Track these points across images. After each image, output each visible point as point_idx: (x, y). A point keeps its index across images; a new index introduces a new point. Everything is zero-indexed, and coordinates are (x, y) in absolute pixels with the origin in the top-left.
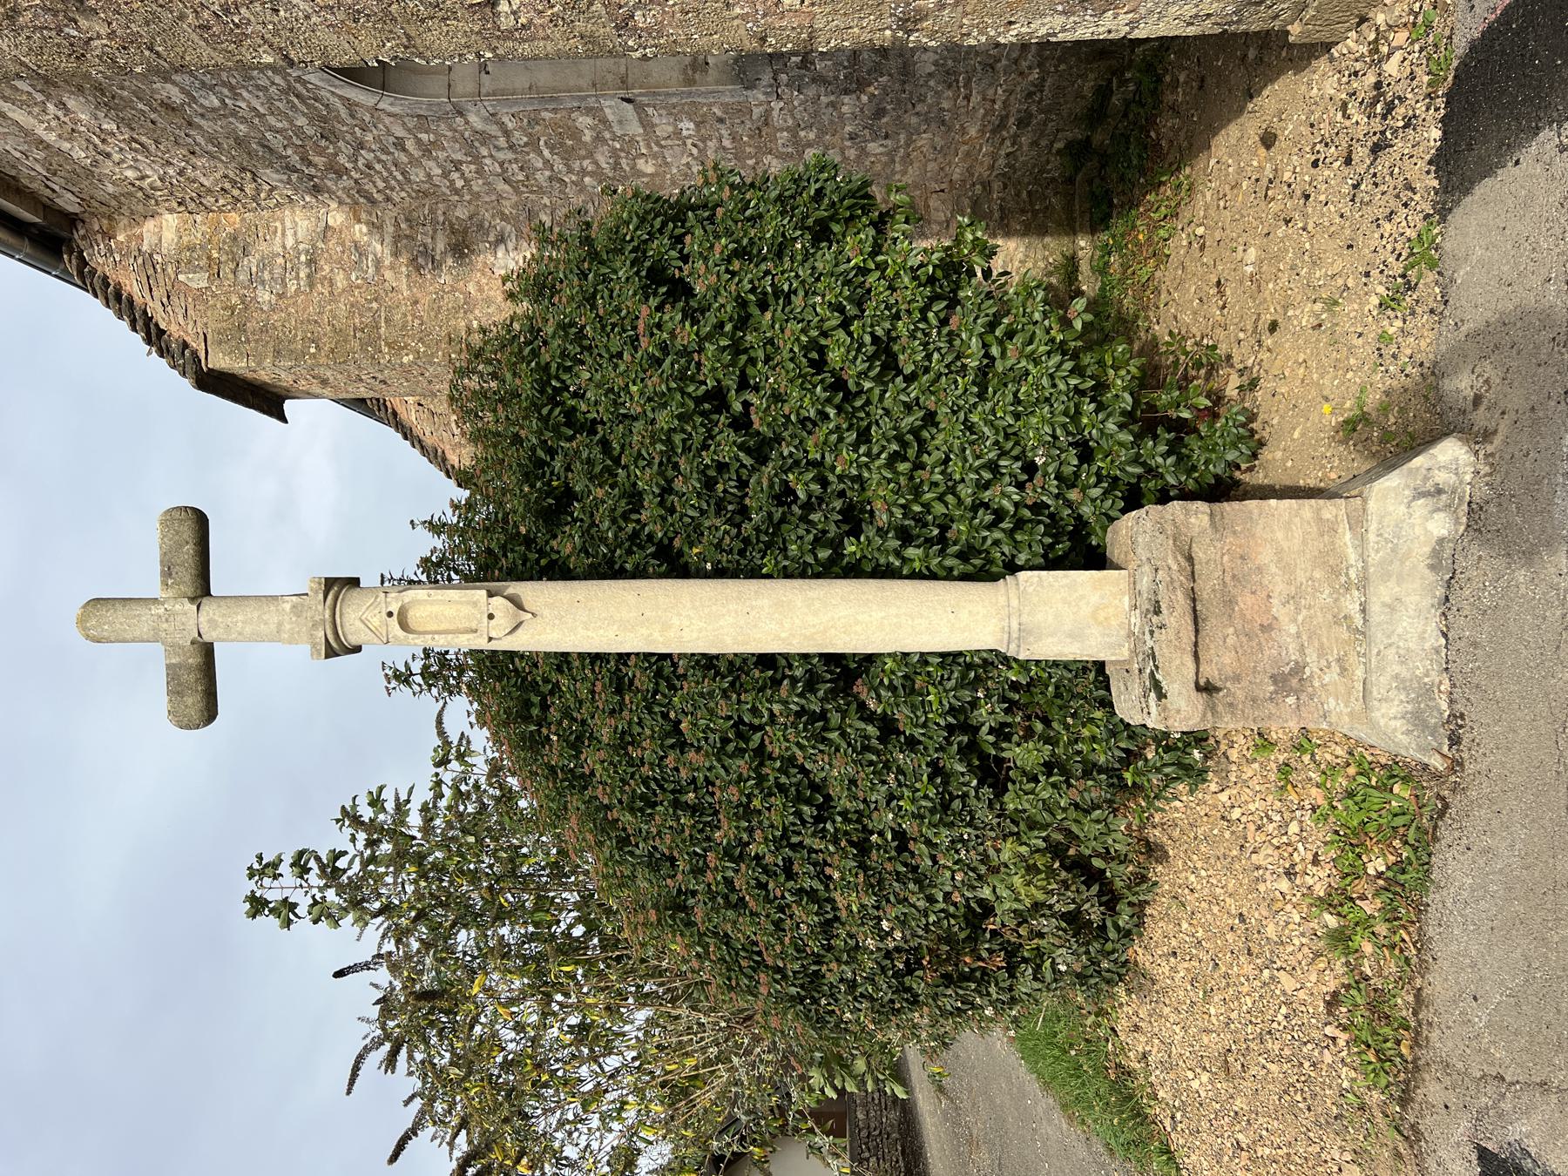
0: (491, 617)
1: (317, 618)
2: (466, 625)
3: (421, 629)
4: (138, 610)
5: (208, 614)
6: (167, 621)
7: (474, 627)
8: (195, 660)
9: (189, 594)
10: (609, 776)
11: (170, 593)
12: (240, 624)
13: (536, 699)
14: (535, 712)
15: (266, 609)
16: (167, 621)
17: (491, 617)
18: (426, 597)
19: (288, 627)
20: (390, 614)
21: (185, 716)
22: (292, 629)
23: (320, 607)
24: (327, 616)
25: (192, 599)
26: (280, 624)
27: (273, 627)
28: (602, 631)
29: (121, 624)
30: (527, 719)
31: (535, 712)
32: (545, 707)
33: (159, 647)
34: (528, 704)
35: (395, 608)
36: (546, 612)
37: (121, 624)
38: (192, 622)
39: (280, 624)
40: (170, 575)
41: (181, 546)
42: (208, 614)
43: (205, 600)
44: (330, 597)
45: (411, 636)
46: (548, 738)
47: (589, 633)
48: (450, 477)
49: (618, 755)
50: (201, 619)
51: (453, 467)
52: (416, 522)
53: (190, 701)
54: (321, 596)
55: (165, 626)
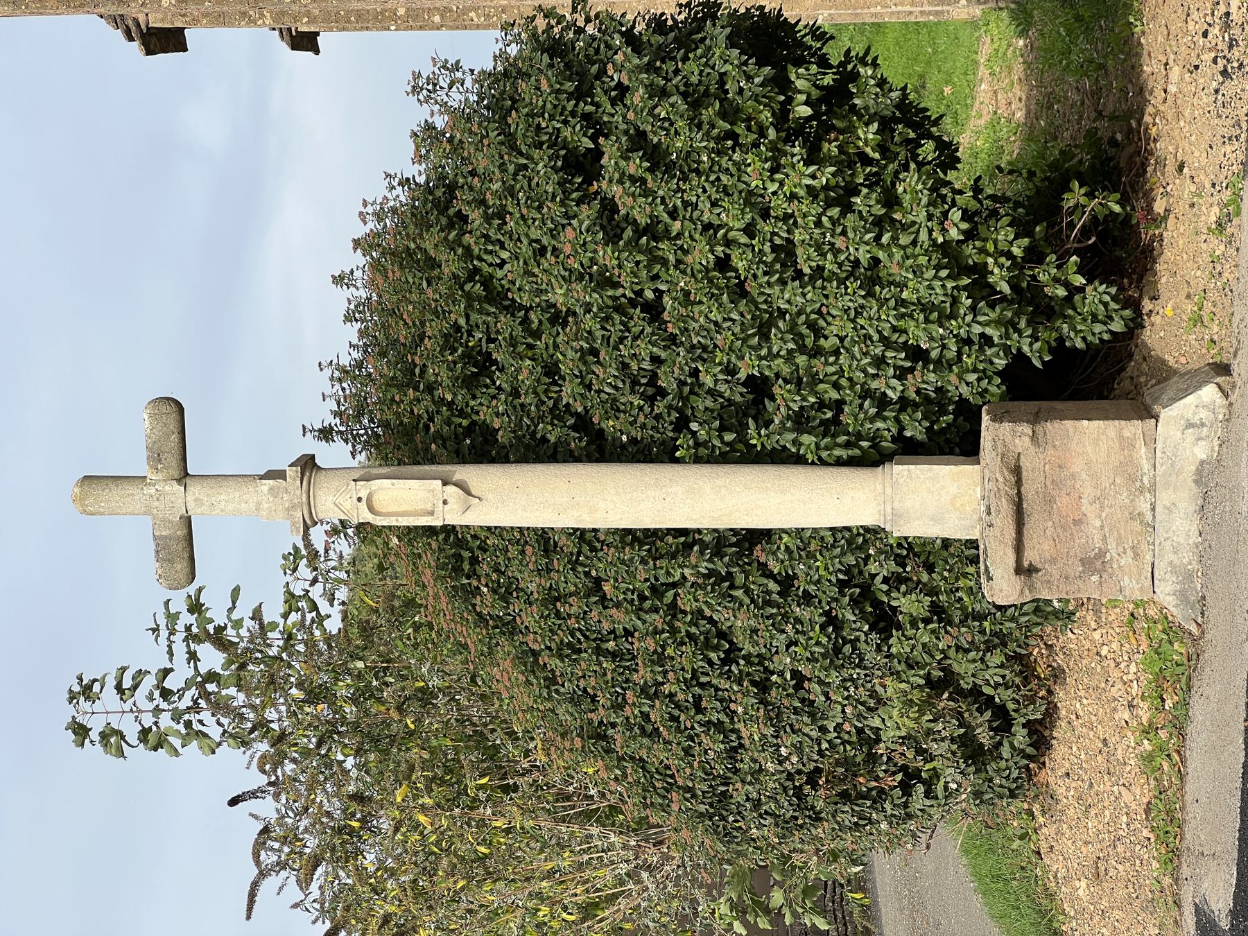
0: (445, 502)
1: (296, 501)
2: (421, 506)
3: (384, 510)
4: (132, 489)
5: (194, 494)
6: (158, 499)
7: (429, 507)
8: (181, 533)
9: (176, 477)
10: (540, 627)
11: (160, 476)
12: (223, 503)
13: (466, 554)
14: (466, 566)
15: (246, 490)
16: (158, 499)
17: (445, 502)
18: (391, 486)
19: (266, 506)
20: (359, 500)
21: (175, 580)
22: (269, 508)
23: (298, 492)
24: (304, 499)
25: (179, 481)
26: (259, 504)
27: (252, 506)
28: (538, 513)
29: (117, 502)
30: (457, 570)
31: (466, 566)
32: (474, 561)
33: (149, 518)
34: (458, 557)
35: (364, 495)
36: (490, 497)
37: (117, 502)
38: (181, 501)
39: (259, 504)
40: (160, 460)
41: (169, 436)
42: (194, 494)
43: (188, 480)
44: (305, 483)
45: (378, 518)
46: (478, 588)
47: (527, 514)
48: (131, 39)
49: (547, 608)
50: (188, 498)
51: (138, 25)
52: (324, 363)
53: (179, 567)
54: (298, 483)
55: (156, 504)
